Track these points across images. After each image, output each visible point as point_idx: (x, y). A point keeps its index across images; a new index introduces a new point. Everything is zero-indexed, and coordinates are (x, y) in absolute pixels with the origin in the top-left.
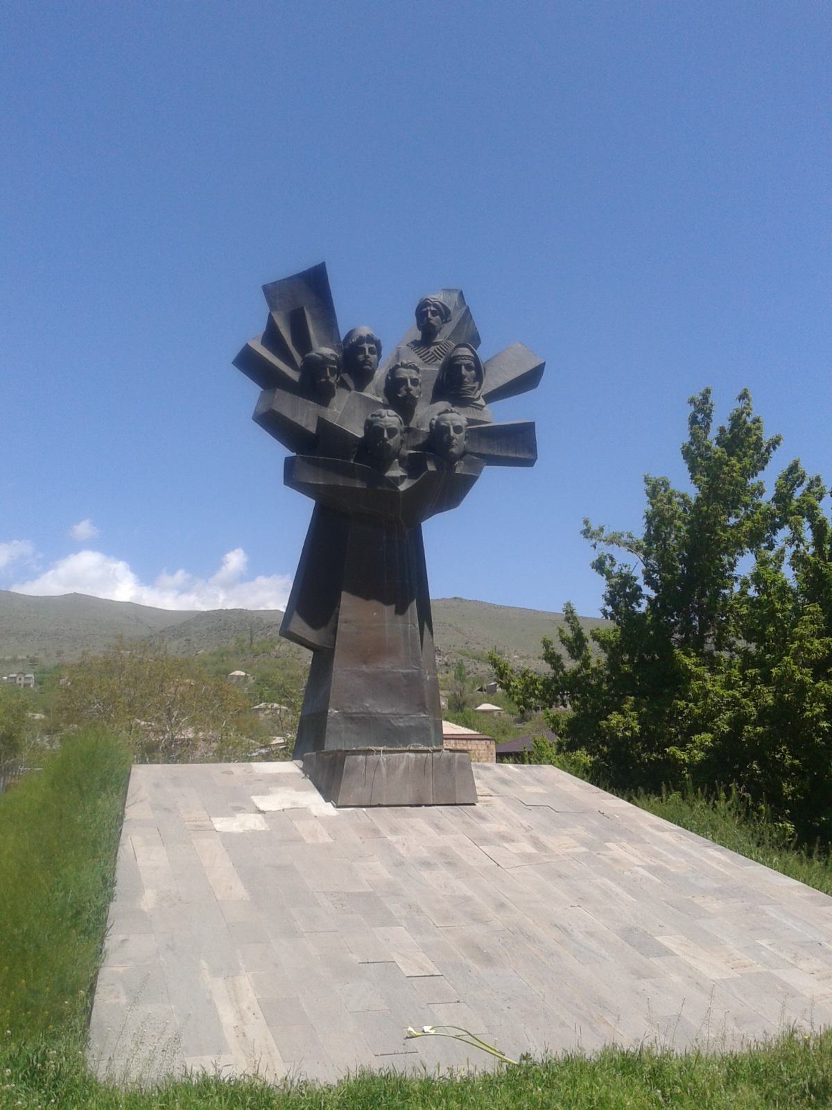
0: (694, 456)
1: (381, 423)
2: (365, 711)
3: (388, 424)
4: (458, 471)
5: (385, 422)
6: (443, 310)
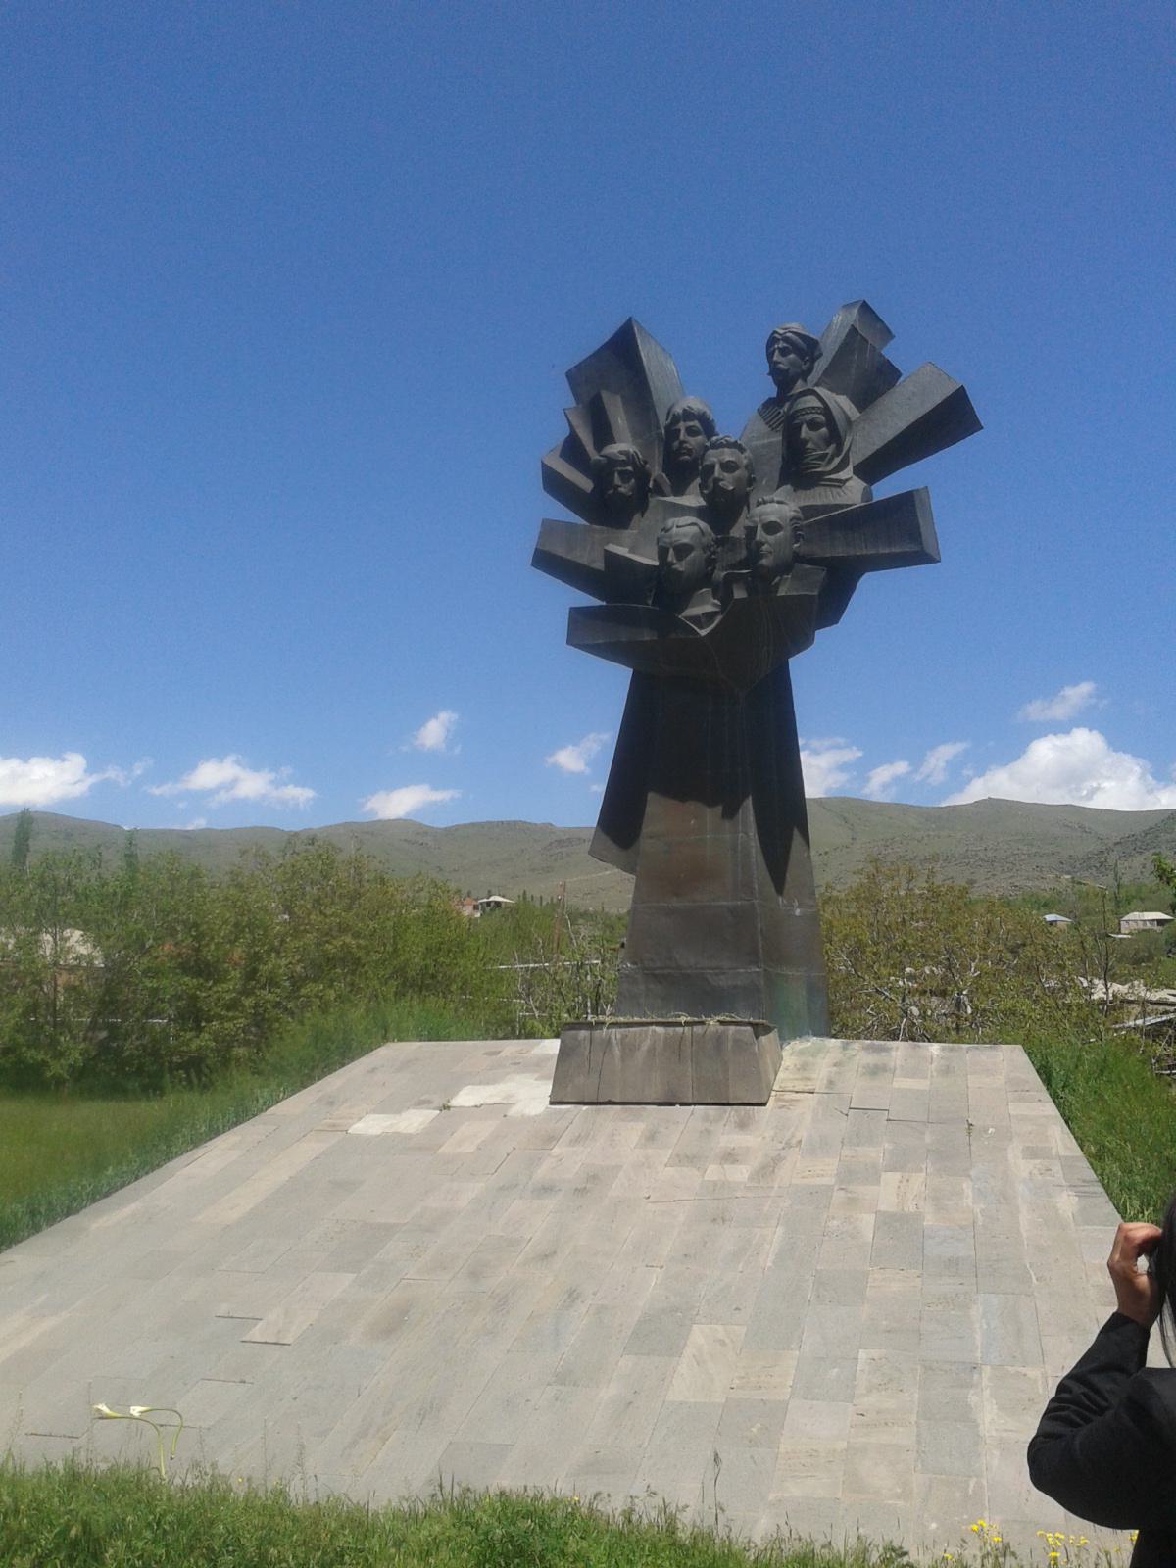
3: (674, 539)
4: (782, 592)
5: (671, 537)
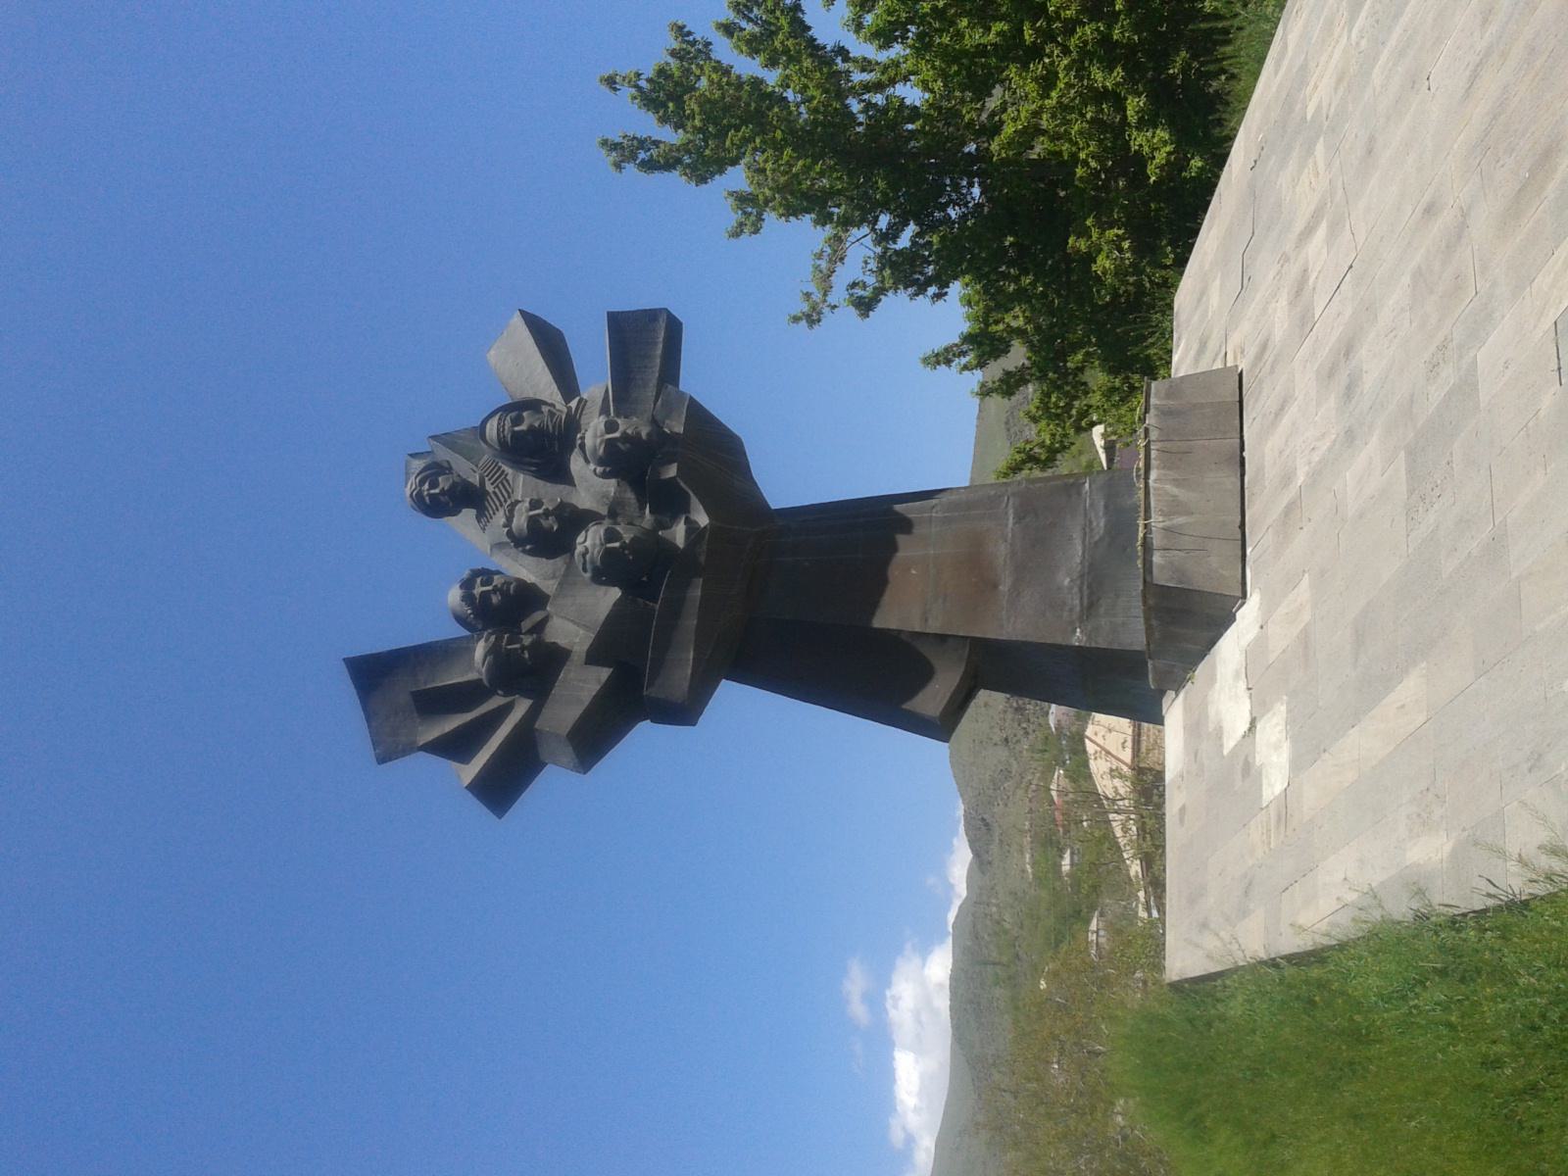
0: (704, 167)
1: (596, 553)
2: (1078, 582)
3: (598, 542)
5: (594, 545)
6: (429, 472)
